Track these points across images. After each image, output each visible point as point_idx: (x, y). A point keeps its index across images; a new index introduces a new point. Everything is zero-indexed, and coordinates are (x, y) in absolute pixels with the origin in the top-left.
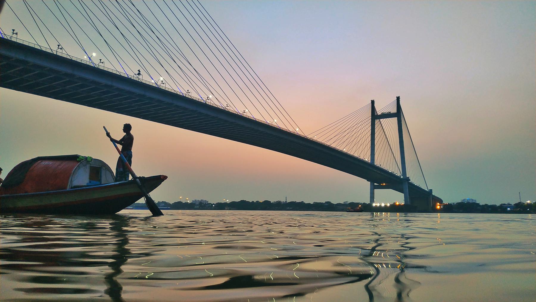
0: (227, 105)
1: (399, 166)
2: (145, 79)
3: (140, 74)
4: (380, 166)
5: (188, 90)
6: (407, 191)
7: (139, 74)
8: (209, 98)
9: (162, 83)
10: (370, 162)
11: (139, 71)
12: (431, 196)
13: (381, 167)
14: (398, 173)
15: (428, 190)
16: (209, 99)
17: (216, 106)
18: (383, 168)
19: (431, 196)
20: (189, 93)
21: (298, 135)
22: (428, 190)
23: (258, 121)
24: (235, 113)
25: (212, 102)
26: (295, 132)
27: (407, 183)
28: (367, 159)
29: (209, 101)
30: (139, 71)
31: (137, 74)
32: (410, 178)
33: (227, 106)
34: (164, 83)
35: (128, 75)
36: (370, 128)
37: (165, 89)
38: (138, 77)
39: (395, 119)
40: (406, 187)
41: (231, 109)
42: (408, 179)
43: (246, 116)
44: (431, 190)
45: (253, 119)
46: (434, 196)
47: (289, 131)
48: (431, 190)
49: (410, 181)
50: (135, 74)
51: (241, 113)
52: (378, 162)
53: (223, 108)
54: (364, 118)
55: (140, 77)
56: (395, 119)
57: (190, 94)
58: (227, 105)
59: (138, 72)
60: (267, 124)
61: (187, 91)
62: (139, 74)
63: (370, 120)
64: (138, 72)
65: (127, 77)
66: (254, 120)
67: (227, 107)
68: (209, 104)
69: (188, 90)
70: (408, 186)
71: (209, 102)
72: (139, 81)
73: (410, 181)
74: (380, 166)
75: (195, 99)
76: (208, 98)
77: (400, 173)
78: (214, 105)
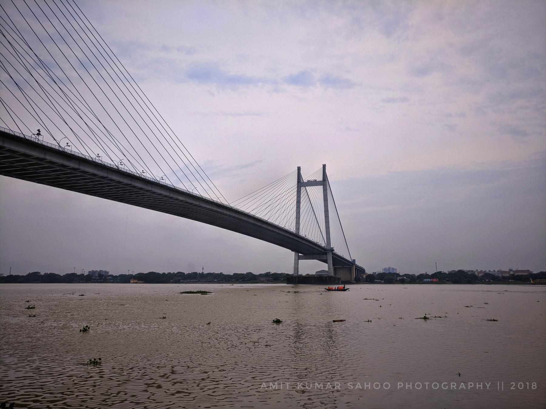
0: (143, 171)
2: (46, 140)
3: (40, 134)
4: (305, 236)
5: (98, 154)
7: (39, 134)
8: (122, 163)
9: (67, 146)
10: (295, 232)
11: (39, 130)
13: (306, 237)
14: (323, 244)
15: (351, 259)
16: (122, 165)
20: (100, 157)
22: (351, 259)
24: (152, 180)
25: (126, 168)
26: (218, 201)
27: (331, 253)
28: (293, 229)
29: (123, 167)
30: (39, 130)
31: (37, 134)
32: (334, 248)
33: (143, 172)
34: (69, 146)
35: (25, 136)
36: (296, 197)
38: (37, 137)
39: (320, 188)
42: (332, 250)
43: (164, 184)
44: (354, 260)
45: (172, 187)
47: (212, 201)
48: (354, 260)
50: (34, 134)
51: (159, 180)
52: (302, 233)
53: (138, 175)
55: (40, 138)
56: (320, 188)
57: (100, 158)
58: (143, 171)
59: (37, 132)
60: (188, 192)
61: (97, 155)
62: (39, 134)
63: (296, 189)
64: (37, 132)
65: (24, 137)
66: (174, 187)
68: (123, 170)
69: (98, 154)
70: (332, 257)
71: (122, 168)
72: (39, 142)
74: (305, 236)
76: (121, 163)
77: (325, 243)
78: (128, 172)
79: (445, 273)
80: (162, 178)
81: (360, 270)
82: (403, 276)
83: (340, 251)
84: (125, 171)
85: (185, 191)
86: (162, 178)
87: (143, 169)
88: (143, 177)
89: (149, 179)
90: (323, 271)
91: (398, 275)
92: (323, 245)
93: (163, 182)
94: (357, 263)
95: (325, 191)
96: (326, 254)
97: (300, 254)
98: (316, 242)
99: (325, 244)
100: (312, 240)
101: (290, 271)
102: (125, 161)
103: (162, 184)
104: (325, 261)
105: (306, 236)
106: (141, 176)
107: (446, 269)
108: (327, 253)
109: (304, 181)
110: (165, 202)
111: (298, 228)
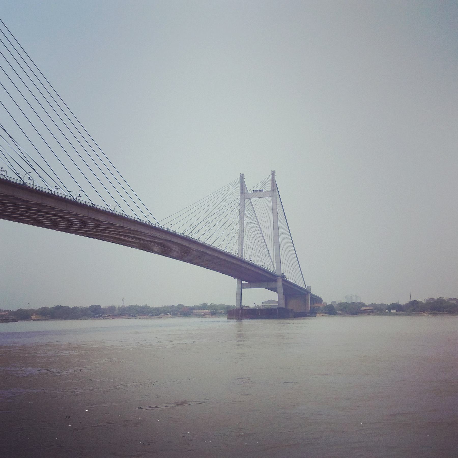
0: (56, 187)
1: (272, 260)
4: (251, 260)
6: (281, 289)
8: (30, 178)
12: (309, 295)
13: (251, 261)
17: (41, 189)
18: (254, 263)
19: (309, 295)
20: (4, 171)
21: (151, 224)
22: (306, 287)
23: (98, 207)
25: (35, 184)
29: (31, 182)
37: (16, 182)
40: (280, 284)
41: (62, 192)
42: (283, 276)
43: (82, 202)
44: (309, 287)
45: (91, 205)
46: (313, 295)
47: (139, 220)
49: (285, 278)
52: (247, 257)
54: (224, 203)
57: (4, 174)
58: (56, 187)
60: (110, 211)
66: (93, 206)
67: (56, 190)
68: (32, 186)
70: (283, 284)
71: (30, 184)
73: (285, 278)
74: (251, 260)
75: (11, 180)
76: (29, 177)
78: (38, 188)
79: (421, 303)
80: (79, 194)
81: (316, 300)
82: (369, 306)
83: (290, 277)
84: (35, 187)
85: (106, 210)
86: (79, 194)
87: (56, 185)
88: (56, 194)
89: (64, 196)
90: (271, 301)
91: (363, 305)
92: (272, 270)
93: (80, 200)
94: (312, 292)
95: (274, 202)
96: (275, 281)
97: (243, 282)
98: (263, 267)
99: (275, 270)
100: (258, 264)
101: (232, 302)
102: (34, 175)
103: (80, 201)
104: (275, 290)
105: (251, 259)
106: (54, 194)
107: (422, 297)
108: (276, 279)
109: (249, 192)
110: (82, 223)
111: (241, 250)
